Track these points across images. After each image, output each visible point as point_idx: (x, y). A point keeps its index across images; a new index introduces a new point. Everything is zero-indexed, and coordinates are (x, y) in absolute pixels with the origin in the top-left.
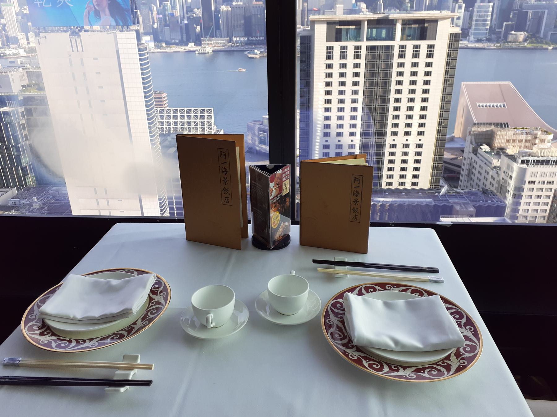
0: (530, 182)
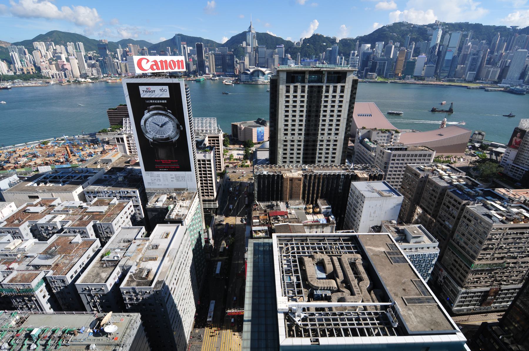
0: (393, 160)
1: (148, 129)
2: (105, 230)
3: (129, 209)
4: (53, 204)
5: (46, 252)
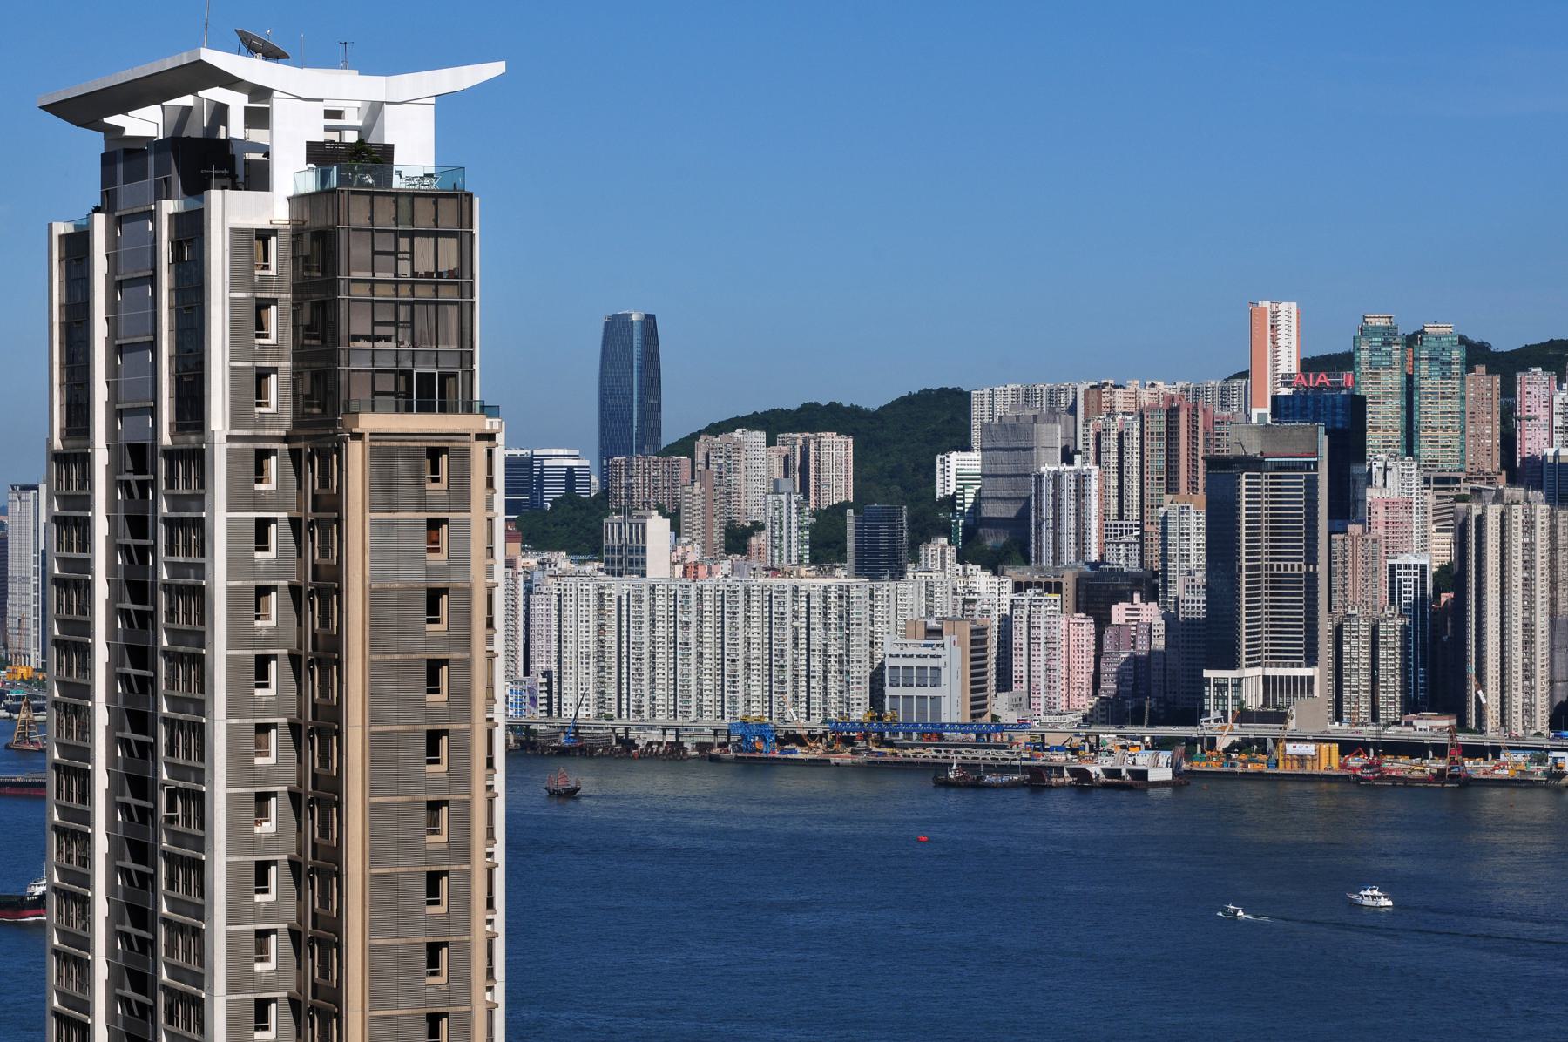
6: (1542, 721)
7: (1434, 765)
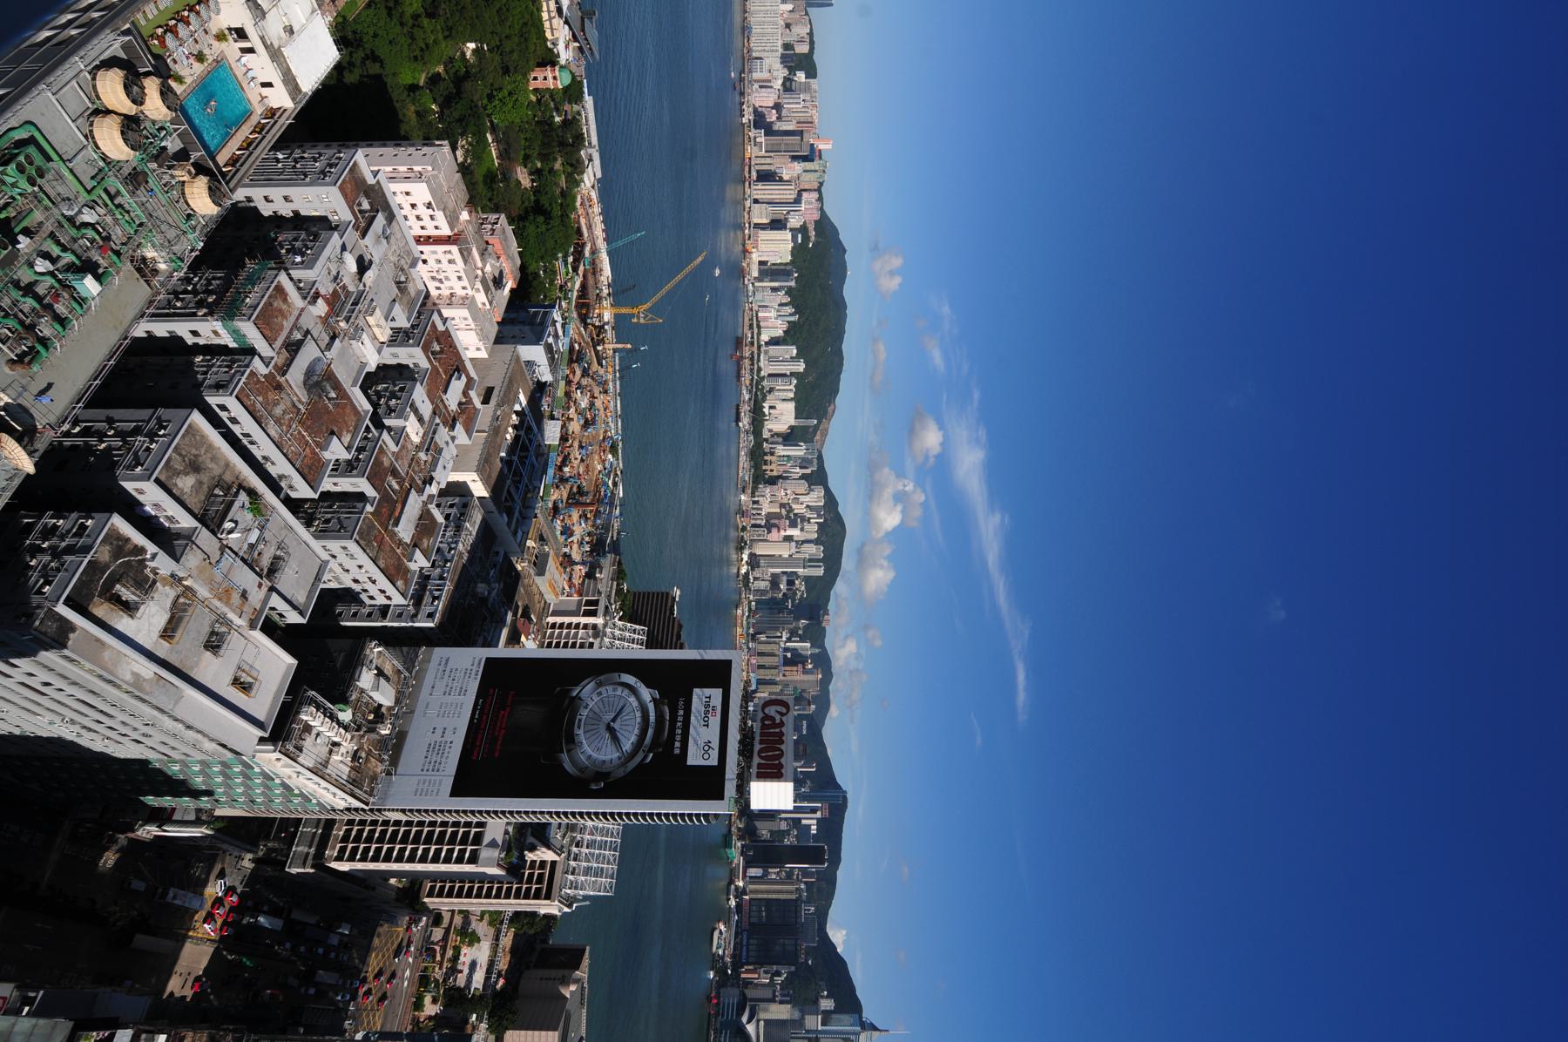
1: (608, 690)
2: (339, 518)
3: (383, 592)
4: (459, 427)
5: (330, 377)
6: (755, 197)
7: (747, 176)
